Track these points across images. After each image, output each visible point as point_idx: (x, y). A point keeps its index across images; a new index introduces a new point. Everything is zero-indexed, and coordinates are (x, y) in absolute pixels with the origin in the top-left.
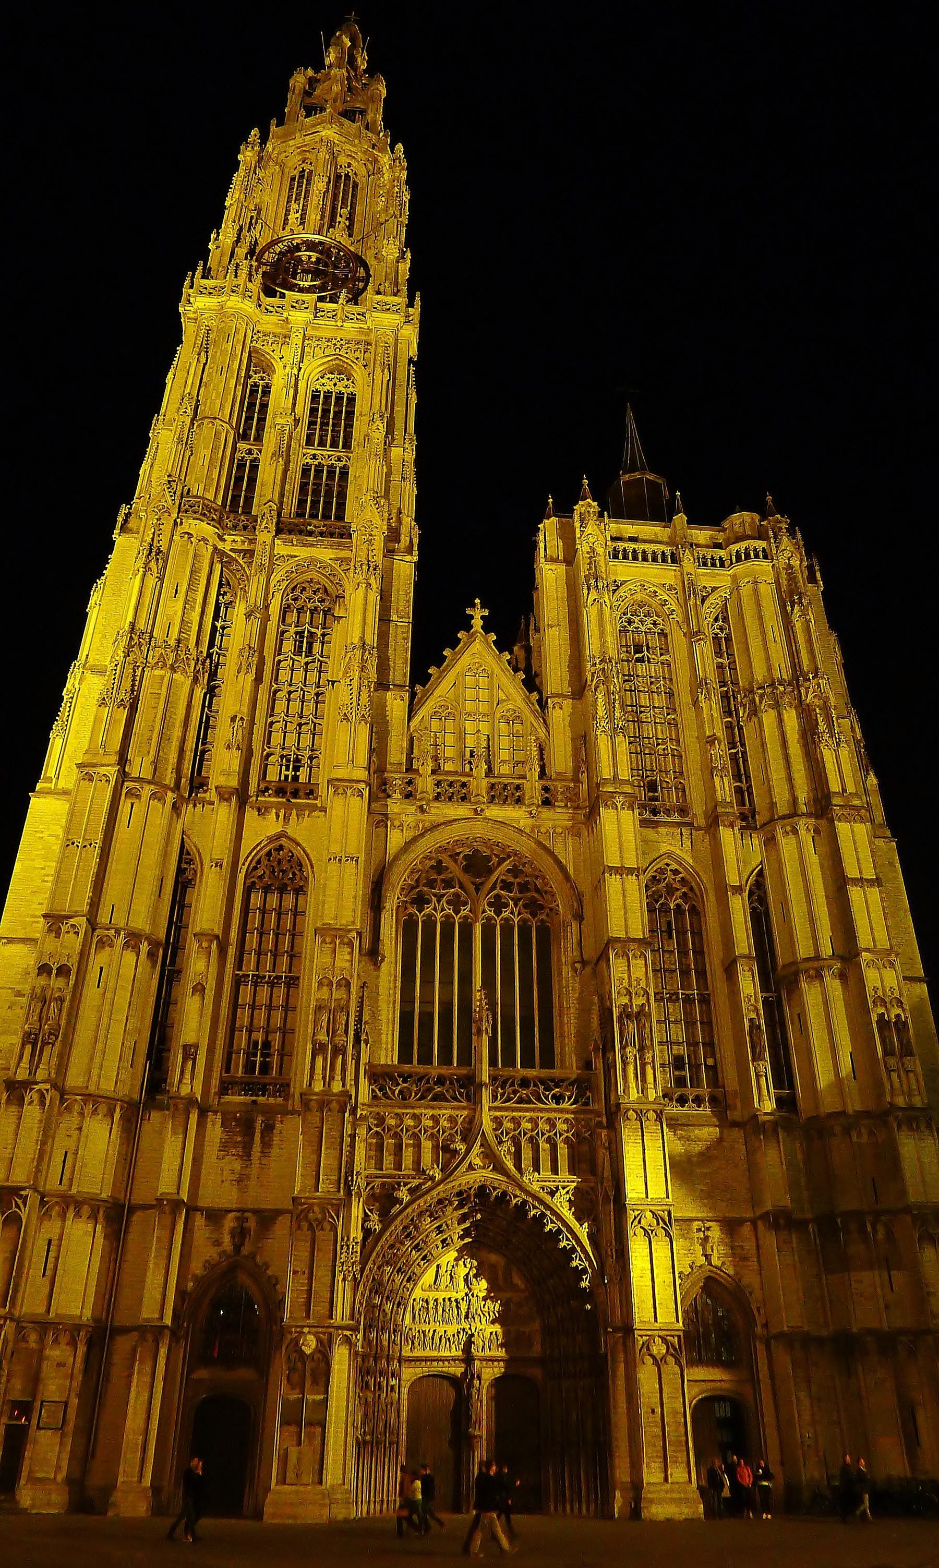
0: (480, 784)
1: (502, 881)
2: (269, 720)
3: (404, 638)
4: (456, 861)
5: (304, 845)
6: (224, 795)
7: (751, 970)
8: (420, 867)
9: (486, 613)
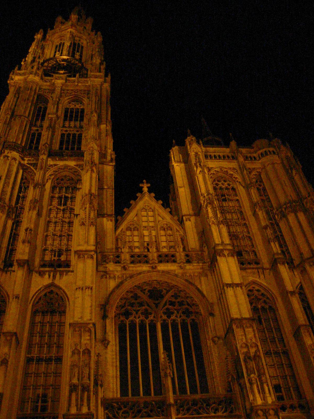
0: (153, 254)
1: (169, 301)
2: (45, 234)
3: (110, 196)
4: (144, 293)
5: (64, 288)
6: (21, 264)
7: (308, 331)
8: (125, 296)
9: (149, 185)
